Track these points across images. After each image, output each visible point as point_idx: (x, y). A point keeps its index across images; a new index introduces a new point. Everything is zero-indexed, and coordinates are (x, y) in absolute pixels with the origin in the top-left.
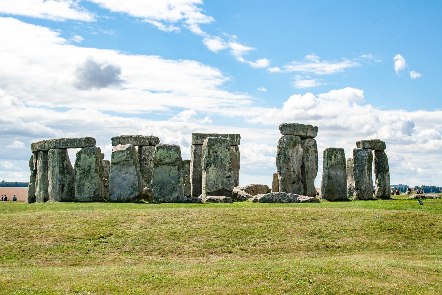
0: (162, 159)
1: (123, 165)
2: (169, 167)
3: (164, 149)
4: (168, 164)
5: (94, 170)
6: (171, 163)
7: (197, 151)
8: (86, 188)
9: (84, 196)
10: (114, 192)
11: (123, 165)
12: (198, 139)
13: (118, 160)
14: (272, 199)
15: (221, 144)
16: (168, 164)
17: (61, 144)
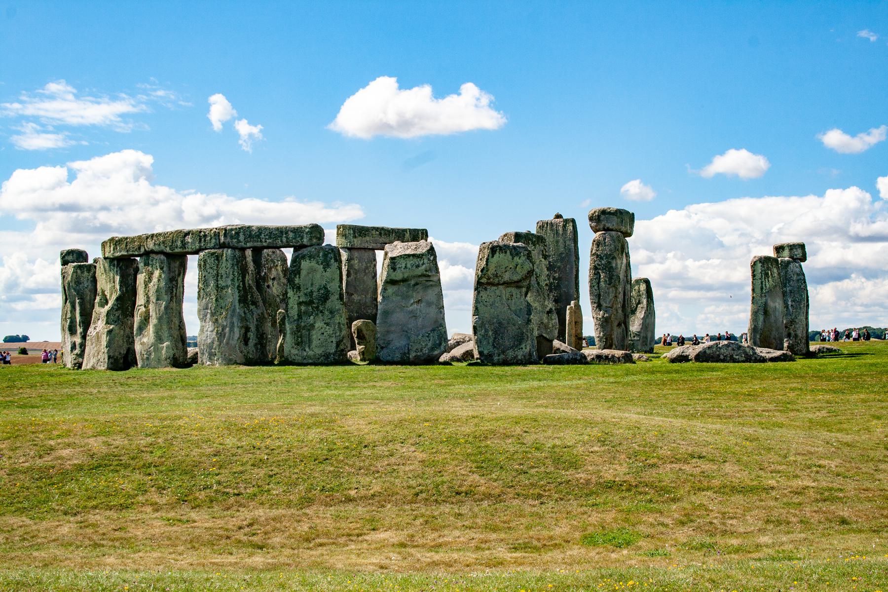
0: (499, 273)
1: (417, 284)
2: (509, 289)
3: (506, 252)
4: (507, 284)
5: (337, 296)
6: (515, 282)
7: (352, 262)
8: (315, 335)
9: (311, 353)
10: (389, 344)
11: (417, 284)
12: (355, 237)
13: (406, 276)
14: (719, 356)
15: (534, 245)
16: (507, 284)
17: (242, 237)
